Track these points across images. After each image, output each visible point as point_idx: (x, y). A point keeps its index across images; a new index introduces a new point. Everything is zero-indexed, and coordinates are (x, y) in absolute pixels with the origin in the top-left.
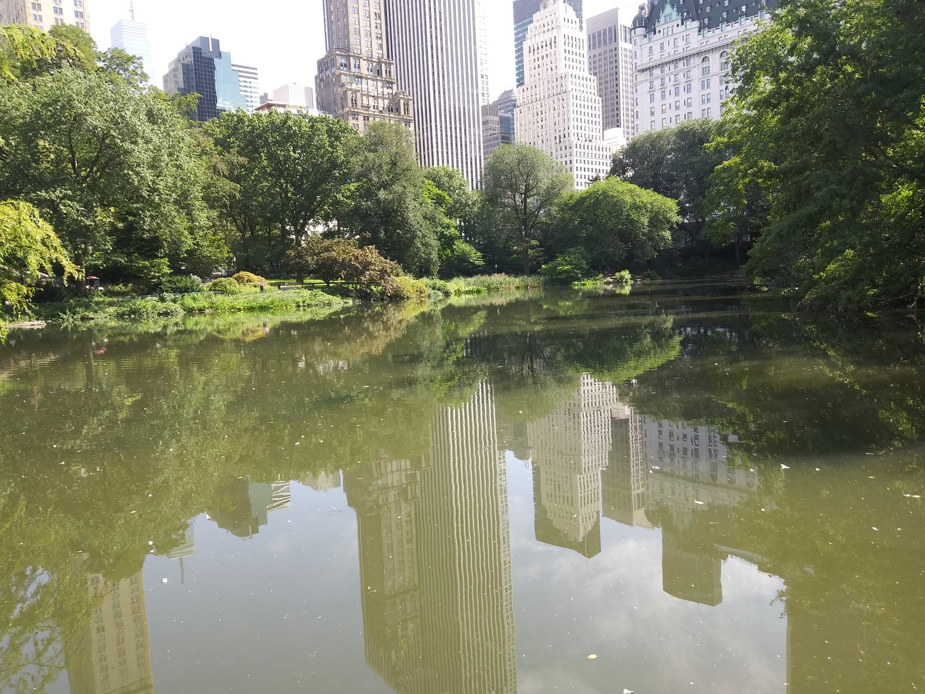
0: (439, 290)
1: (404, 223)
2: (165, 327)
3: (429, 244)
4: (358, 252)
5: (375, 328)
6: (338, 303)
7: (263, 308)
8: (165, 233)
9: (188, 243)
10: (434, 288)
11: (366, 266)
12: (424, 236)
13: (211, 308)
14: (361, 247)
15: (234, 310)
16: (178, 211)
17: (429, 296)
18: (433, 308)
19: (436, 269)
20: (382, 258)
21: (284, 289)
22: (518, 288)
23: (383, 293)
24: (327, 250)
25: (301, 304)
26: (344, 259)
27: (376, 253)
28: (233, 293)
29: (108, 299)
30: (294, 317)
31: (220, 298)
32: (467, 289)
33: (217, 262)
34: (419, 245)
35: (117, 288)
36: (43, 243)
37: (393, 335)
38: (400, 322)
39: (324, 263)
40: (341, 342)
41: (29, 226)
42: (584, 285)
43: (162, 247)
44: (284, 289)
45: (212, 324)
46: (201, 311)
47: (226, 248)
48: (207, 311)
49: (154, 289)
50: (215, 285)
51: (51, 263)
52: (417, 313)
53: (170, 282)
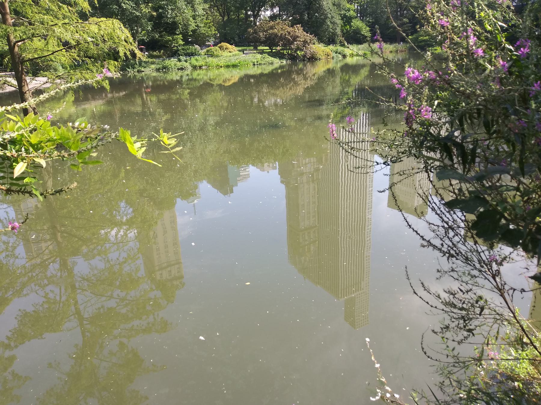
0: (340, 53)
1: (320, 8)
2: (181, 77)
3: (335, 22)
4: (291, 29)
6: (277, 62)
7: (234, 66)
9: (192, 26)
10: (336, 53)
11: (295, 38)
12: (332, 17)
13: (206, 65)
14: (292, 26)
15: (219, 67)
16: (186, 5)
17: (333, 58)
18: (335, 65)
21: (246, 54)
22: (391, 52)
23: (304, 56)
24: (272, 28)
25: (256, 63)
26: (281, 34)
27: (301, 29)
28: (217, 56)
29: (150, 60)
31: (210, 59)
33: (208, 36)
34: (329, 23)
35: (155, 53)
36: (126, 42)
37: (309, 83)
38: (314, 75)
39: (270, 37)
40: (278, 88)
41: (118, 32)
42: (436, 50)
43: (178, 28)
45: (207, 75)
46: (200, 67)
47: (214, 28)
49: (174, 54)
50: (208, 51)
51: (130, 51)
52: (325, 69)
53: (183, 49)
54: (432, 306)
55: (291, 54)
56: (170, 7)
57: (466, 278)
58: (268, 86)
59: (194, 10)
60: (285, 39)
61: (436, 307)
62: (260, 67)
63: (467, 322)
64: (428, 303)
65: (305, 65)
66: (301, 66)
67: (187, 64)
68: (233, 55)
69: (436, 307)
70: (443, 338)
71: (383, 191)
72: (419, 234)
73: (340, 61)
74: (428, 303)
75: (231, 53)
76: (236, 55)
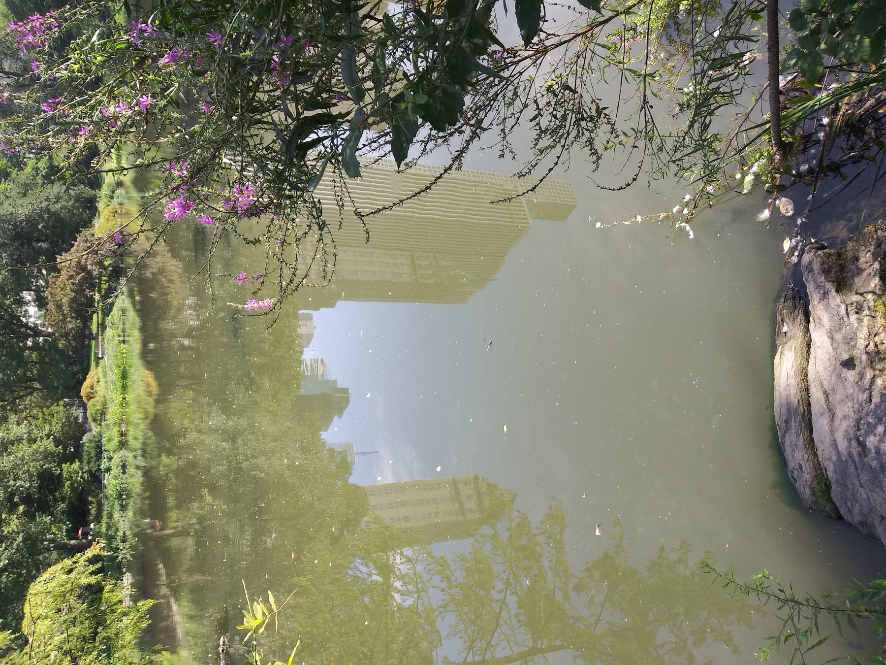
0: (113, 192)
2: (138, 467)
3: (55, 197)
4: (64, 275)
5: (154, 264)
6: (122, 301)
7: (124, 376)
8: (34, 467)
10: (112, 198)
12: (47, 199)
13: (120, 424)
14: (59, 271)
15: (124, 403)
16: (10, 454)
17: (121, 204)
19: (88, 191)
20: (72, 250)
21: (103, 353)
24: (59, 307)
25: (121, 338)
26: (72, 291)
28: (105, 404)
29: (105, 519)
30: (135, 346)
31: (108, 417)
32: (115, 161)
33: (68, 418)
34: (58, 206)
35: (93, 511)
36: (70, 571)
39: (76, 311)
40: (167, 305)
44: (103, 353)
45: (138, 424)
46: (122, 434)
47: (53, 408)
48: (123, 429)
49: (96, 479)
50: (95, 420)
53: (89, 463)
54: (556, 164)
55: (110, 276)
56: (12, 483)
57: (518, 105)
58: (163, 320)
59: (19, 440)
60: (80, 284)
61: (558, 157)
62: (128, 331)
63: (585, 116)
64: (550, 170)
65: (130, 254)
66: (131, 261)
67: (115, 456)
68: (105, 376)
69: (558, 157)
70: (606, 148)
71: (367, 233)
72: (441, 175)
73: (127, 192)
74: (550, 170)
75: (100, 381)
76: (105, 372)
